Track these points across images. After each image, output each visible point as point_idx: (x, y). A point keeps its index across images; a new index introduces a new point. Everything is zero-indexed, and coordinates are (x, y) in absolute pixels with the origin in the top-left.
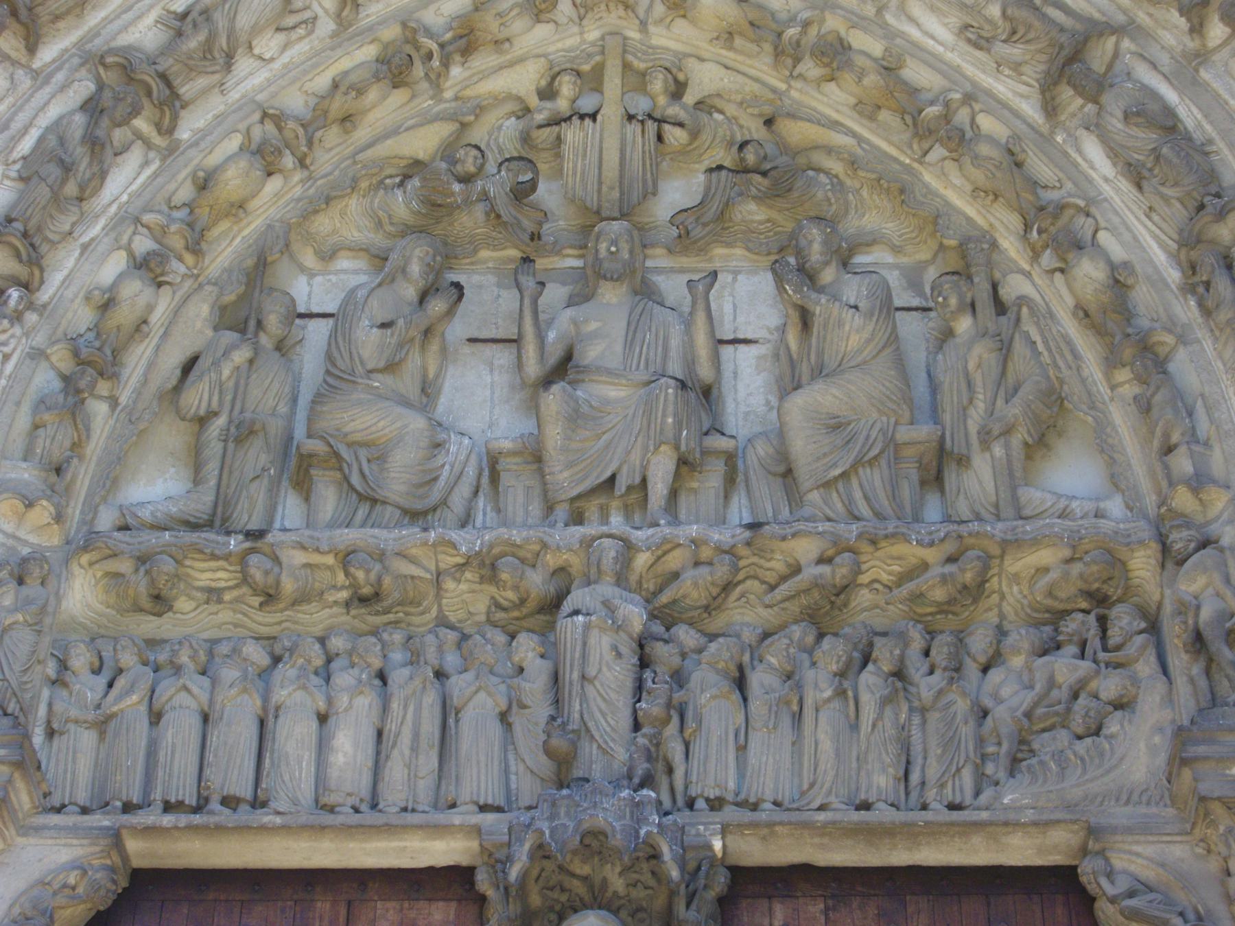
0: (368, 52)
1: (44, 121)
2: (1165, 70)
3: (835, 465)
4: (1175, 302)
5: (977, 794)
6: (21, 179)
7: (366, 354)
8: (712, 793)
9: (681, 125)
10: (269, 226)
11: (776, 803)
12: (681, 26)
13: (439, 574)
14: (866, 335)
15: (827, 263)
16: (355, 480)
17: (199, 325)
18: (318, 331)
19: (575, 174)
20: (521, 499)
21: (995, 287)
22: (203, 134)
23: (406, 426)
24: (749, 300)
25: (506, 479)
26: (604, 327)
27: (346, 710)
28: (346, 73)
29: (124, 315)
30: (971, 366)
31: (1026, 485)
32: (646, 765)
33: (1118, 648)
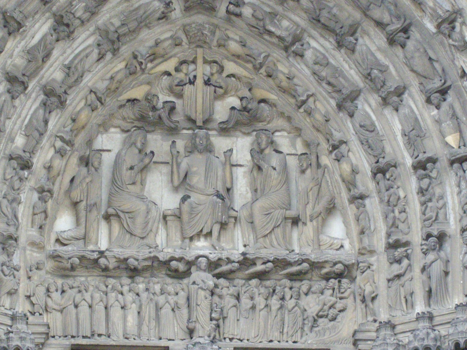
0: (122, 65)
2: (374, 108)
3: (267, 229)
4: (369, 182)
5: (302, 336)
6: (26, 135)
8: (231, 337)
11: (248, 340)
14: (279, 181)
16: (125, 225)
17: (74, 166)
18: (108, 159)
19: (187, 105)
20: (174, 231)
21: (317, 157)
25: (169, 223)
26: (197, 163)
27: (130, 309)
32: (214, 333)
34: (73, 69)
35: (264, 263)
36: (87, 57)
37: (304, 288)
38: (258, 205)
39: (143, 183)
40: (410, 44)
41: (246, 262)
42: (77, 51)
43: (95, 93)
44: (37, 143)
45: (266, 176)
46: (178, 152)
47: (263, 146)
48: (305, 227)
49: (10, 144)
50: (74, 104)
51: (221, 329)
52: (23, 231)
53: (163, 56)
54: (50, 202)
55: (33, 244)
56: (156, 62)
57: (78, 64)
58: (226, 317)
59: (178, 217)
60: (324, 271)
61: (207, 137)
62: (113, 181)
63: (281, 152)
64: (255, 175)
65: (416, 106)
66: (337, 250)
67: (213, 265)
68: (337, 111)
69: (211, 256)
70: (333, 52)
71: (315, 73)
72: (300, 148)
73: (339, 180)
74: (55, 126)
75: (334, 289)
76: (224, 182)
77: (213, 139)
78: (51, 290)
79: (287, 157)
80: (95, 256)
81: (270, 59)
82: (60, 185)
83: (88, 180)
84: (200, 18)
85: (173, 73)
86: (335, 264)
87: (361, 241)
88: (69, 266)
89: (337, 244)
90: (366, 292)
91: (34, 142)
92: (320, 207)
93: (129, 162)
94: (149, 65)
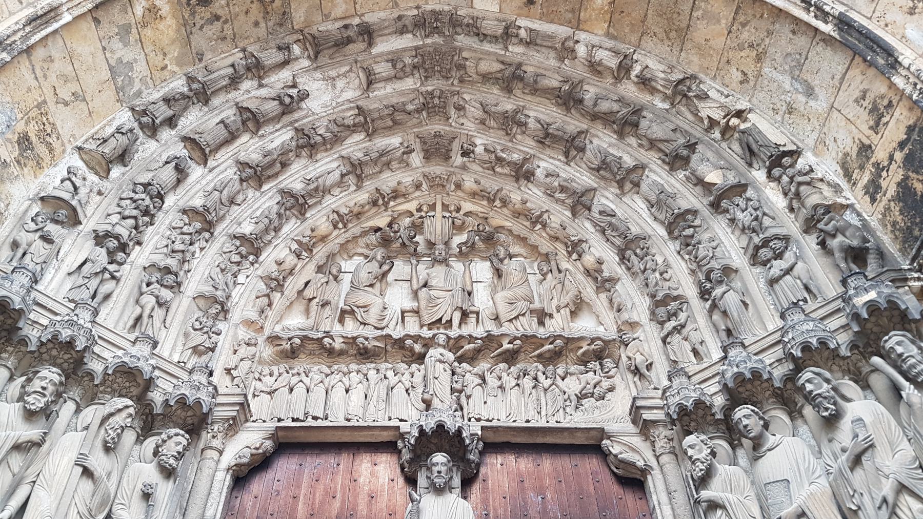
0: (367, 195)
1: (264, 207)
16: (359, 318)
24: (482, 269)
29: (286, 266)
33: (607, 372)
37: (560, 371)
40: (644, 124)
41: (490, 340)
43: (337, 213)
48: (553, 321)
49: (235, 226)
51: (465, 410)
55: (249, 323)
56: (398, 201)
58: (470, 396)
60: (581, 351)
65: (660, 177)
67: (454, 345)
75: (595, 372)
78: (263, 373)
80: (320, 335)
81: (504, 192)
84: (437, 169)
85: (415, 212)
88: (288, 346)
90: (637, 361)
91: (261, 226)
92: (566, 299)
94: (392, 203)
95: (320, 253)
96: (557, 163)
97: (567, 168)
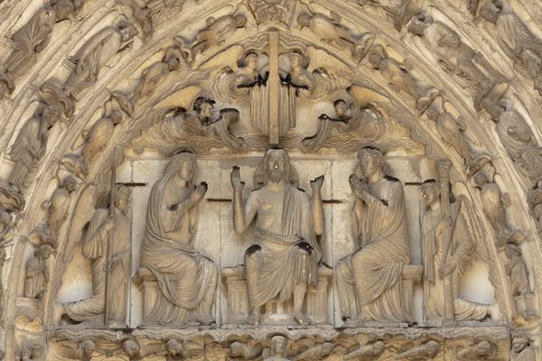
0: (158, 57)
2: (528, 107)
3: (375, 292)
7: (165, 224)
9: (306, 87)
10: (115, 148)
12: (306, 31)
13: (205, 345)
14: (392, 221)
15: (373, 173)
17: (88, 206)
18: (140, 197)
20: (237, 299)
21: (450, 186)
22: (85, 109)
23: (186, 267)
25: (231, 288)
26: (271, 201)
28: (150, 68)
30: (437, 234)
31: (458, 297)
34: (81, 63)
35: (371, 342)
36: (102, 43)
38: (362, 256)
39: (192, 230)
42: (87, 38)
44: (30, 171)
45: (373, 214)
46: (243, 183)
47: (369, 171)
50: (86, 116)
52: (10, 301)
53: (219, 44)
54: (52, 257)
56: (209, 52)
57: (90, 54)
59: (244, 278)
61: (287, 160)
62: (147, 230)
63: (397, 180)
64: (358, 213)
66: (481, 321)
68: (476, 114)
69: (291, 333)
70: (466, 27)
71: (441, 61)
72: (425, 172)
73: (483, 217)
74: (58, 147)
76: (312, 227)
77: (296, 164)
79: (406, 188)
80: (119, 336)
82: (68, 235)
83: (109, 227)
85: (235, 68)
86: (476, 342)
87: (516, 305)
89: (481, 311)
92: (453, 261)
93: (169, 199)
95: (96, 167)
96: (458, 17)
97: (470, 29)
